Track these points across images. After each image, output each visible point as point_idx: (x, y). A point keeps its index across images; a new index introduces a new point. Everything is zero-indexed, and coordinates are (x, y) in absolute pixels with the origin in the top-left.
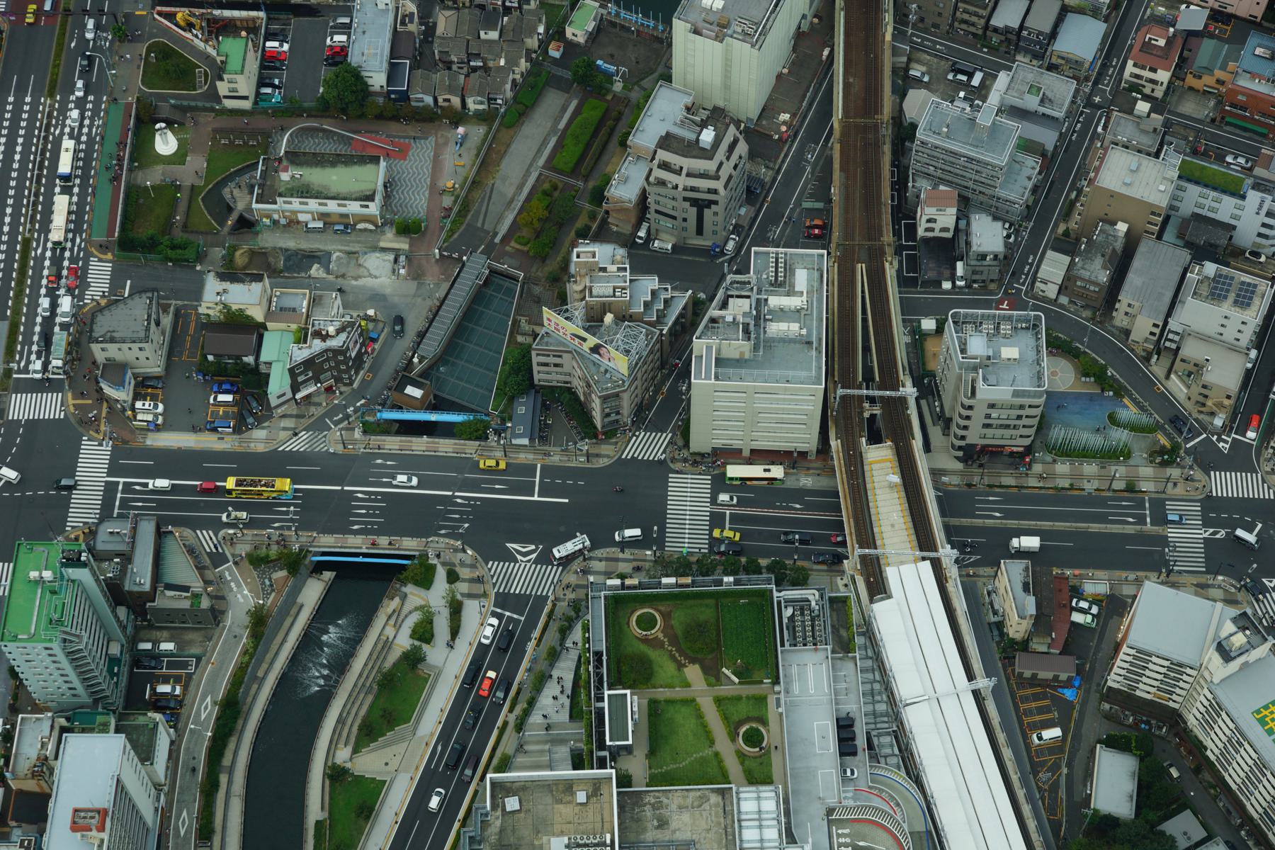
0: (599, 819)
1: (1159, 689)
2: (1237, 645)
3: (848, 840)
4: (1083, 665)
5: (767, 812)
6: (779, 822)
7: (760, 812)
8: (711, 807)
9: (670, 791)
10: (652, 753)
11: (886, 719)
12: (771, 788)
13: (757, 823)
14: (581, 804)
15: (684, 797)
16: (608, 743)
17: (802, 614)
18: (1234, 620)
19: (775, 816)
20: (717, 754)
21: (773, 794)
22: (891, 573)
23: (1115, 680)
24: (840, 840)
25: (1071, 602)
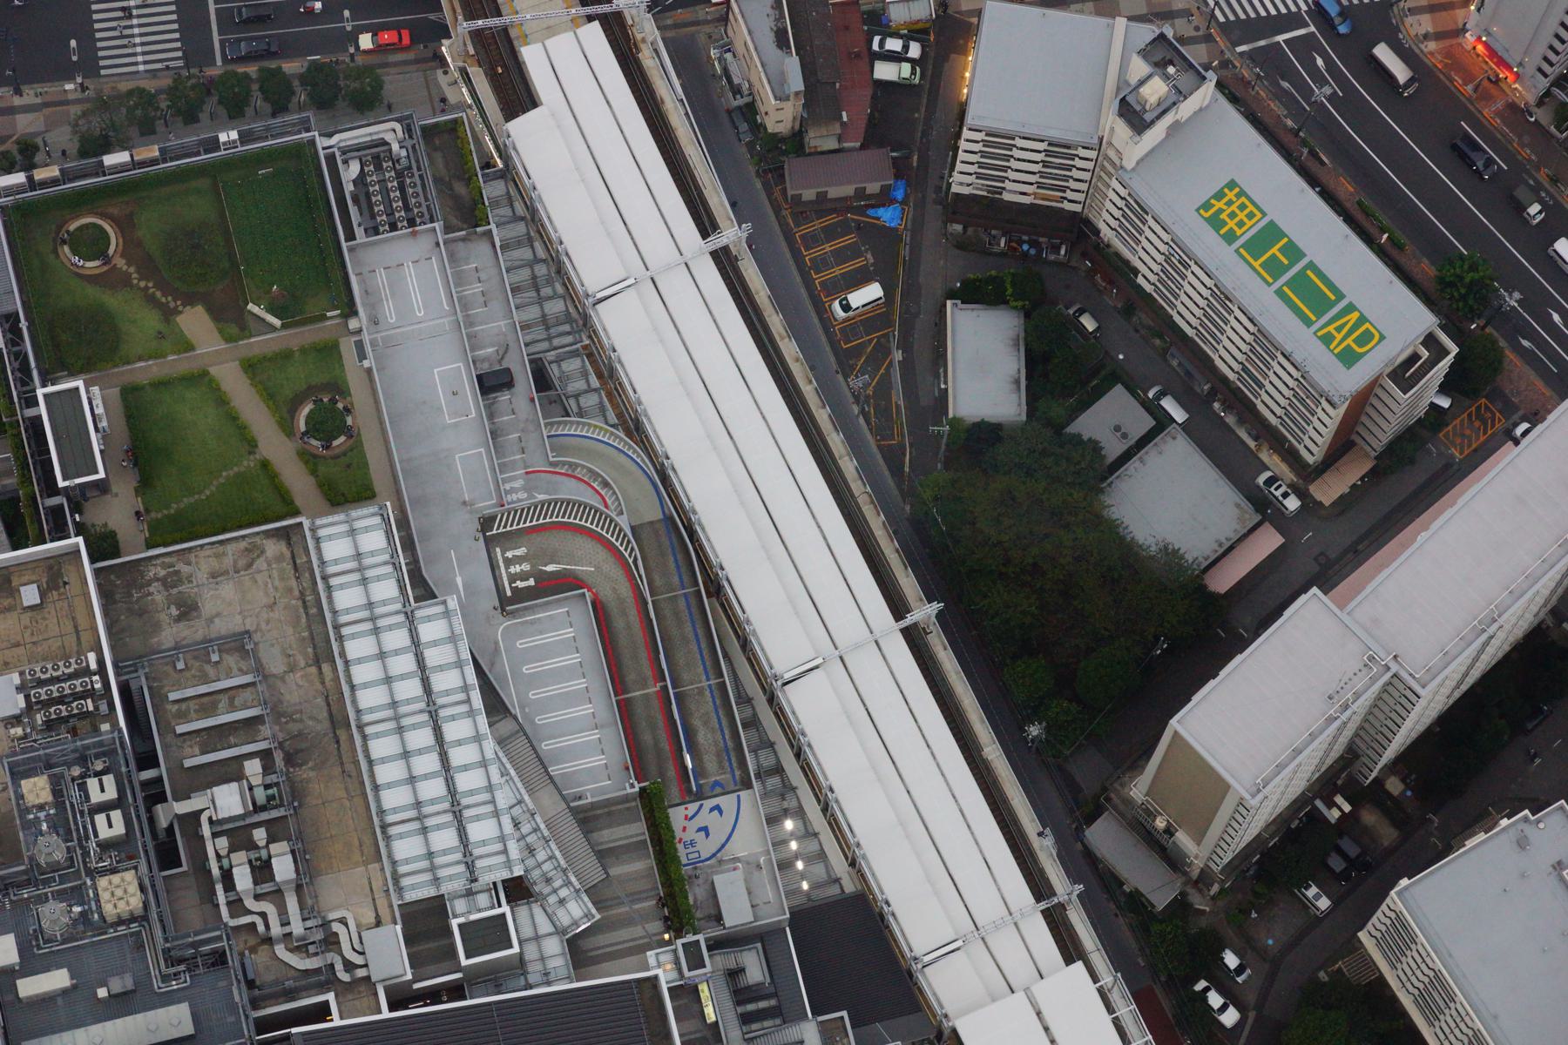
0: (69, 627)
1: (1040, 186)
2: (1153, 100)
3: (526, 567)
4: (908, 157)
5: (372, 553)
6: (397, 567)
7: (358, 556)
8: (269, 565)
9: (190, 549)
10: (145, 485)
11: (567, 328)
12: (373, 509)
13: (356, 576)
14: (32, 608)
15: (217, 556)
16: (61, 484)
17: (379, 167)
18: (1144, 54)
19: (386, 557)
20: (265, 464)
21: (377, 520)
22: (531, 56)
23: (963, 181)
24: (512, 570)
25: (870, 42)
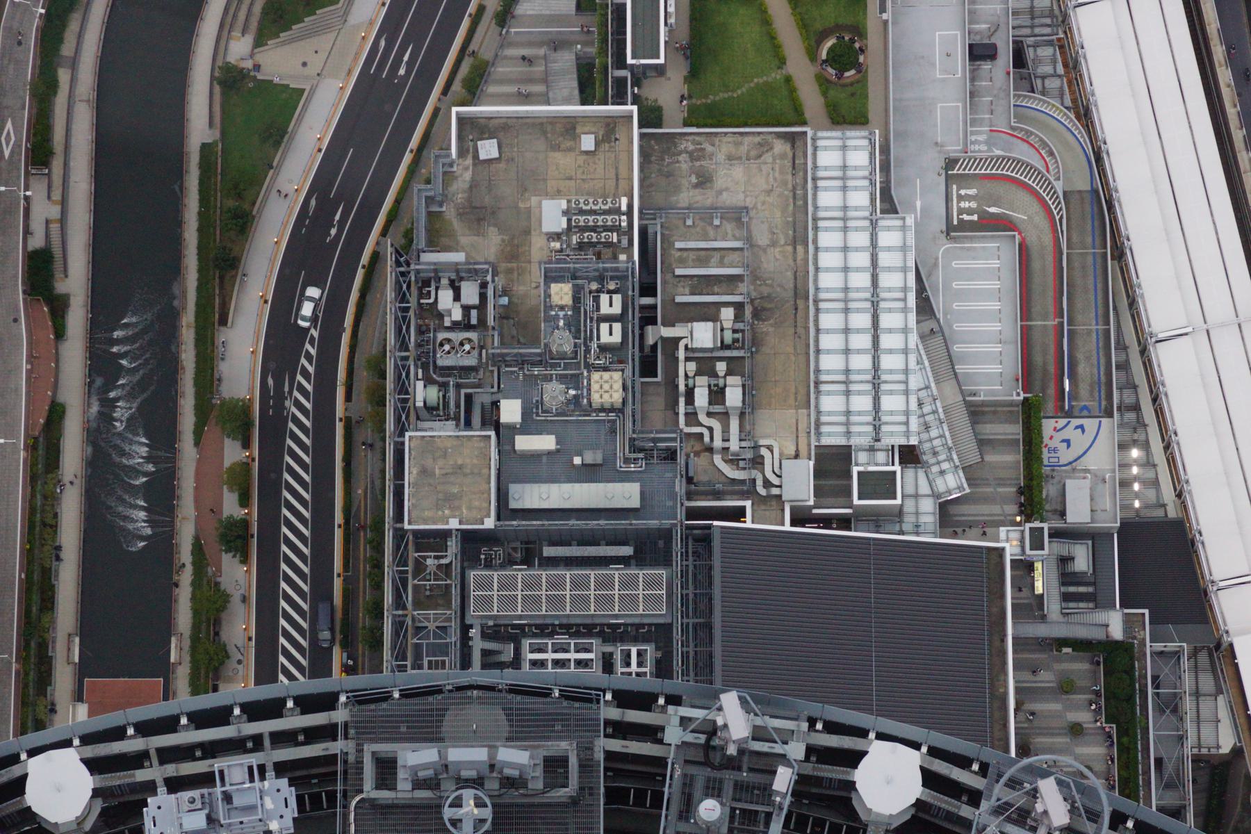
0: (613, 175)
3: (973, 205)
5: (856, 168)
6: (872, 183)
7: (844, 167)
8: (774, 159)
9: (716, 134)
10: (693, 75)
11: (1048, 21)
12: (865, 133)
13: (839, 183)
14: (587, 153)
15: (738, 144)
16: (630, 61)
19: (866, 173)
20: (788, 80)
21: (866, 142)
24: (962, 205)
